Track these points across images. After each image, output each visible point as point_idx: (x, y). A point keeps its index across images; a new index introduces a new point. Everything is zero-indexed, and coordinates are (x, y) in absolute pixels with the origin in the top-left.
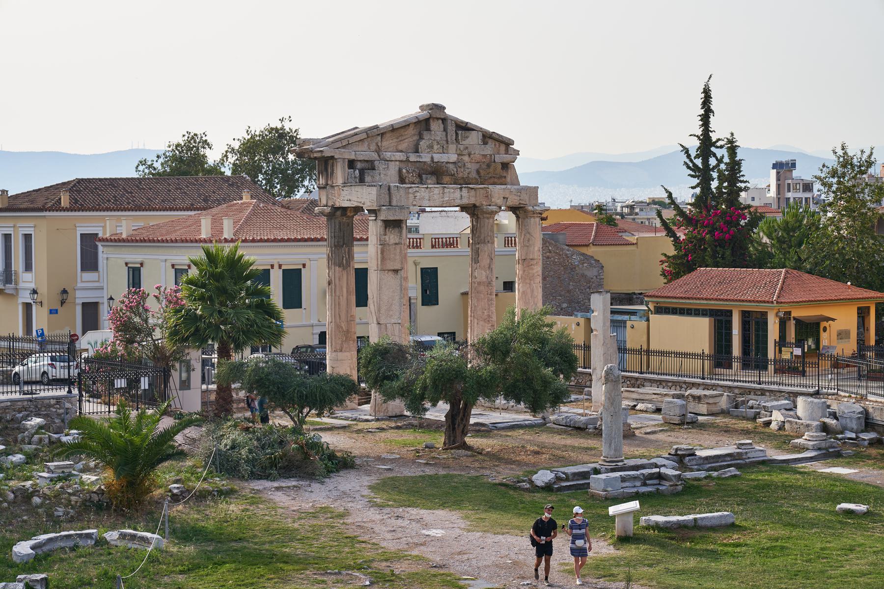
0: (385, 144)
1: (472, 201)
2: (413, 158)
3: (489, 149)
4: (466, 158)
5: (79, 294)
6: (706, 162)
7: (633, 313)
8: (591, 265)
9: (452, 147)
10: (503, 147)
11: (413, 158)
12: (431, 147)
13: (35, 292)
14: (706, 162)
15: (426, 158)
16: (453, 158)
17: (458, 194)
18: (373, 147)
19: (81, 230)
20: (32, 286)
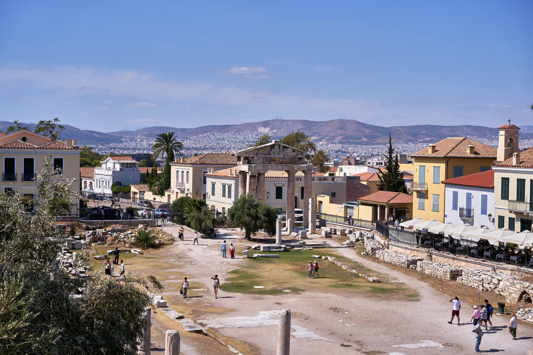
0: (259, 152)
1: (287, 169)
2: (268, 156)
3: (294, 154)
4: (286, 156)
5: (202, 191)
6: (391, 156)
7: (355, 204)
8: (365, 188)
9: (282, 153)
10: (300, 153)
11: (268, 156)
12: (274, 153)
13: (188, 190)
14: (391, 156)
15: (272, 156)
16: (282, 156)
17: (282, 167)
18: (255, 153)
19: (203, 171)
20: (188, 188)
